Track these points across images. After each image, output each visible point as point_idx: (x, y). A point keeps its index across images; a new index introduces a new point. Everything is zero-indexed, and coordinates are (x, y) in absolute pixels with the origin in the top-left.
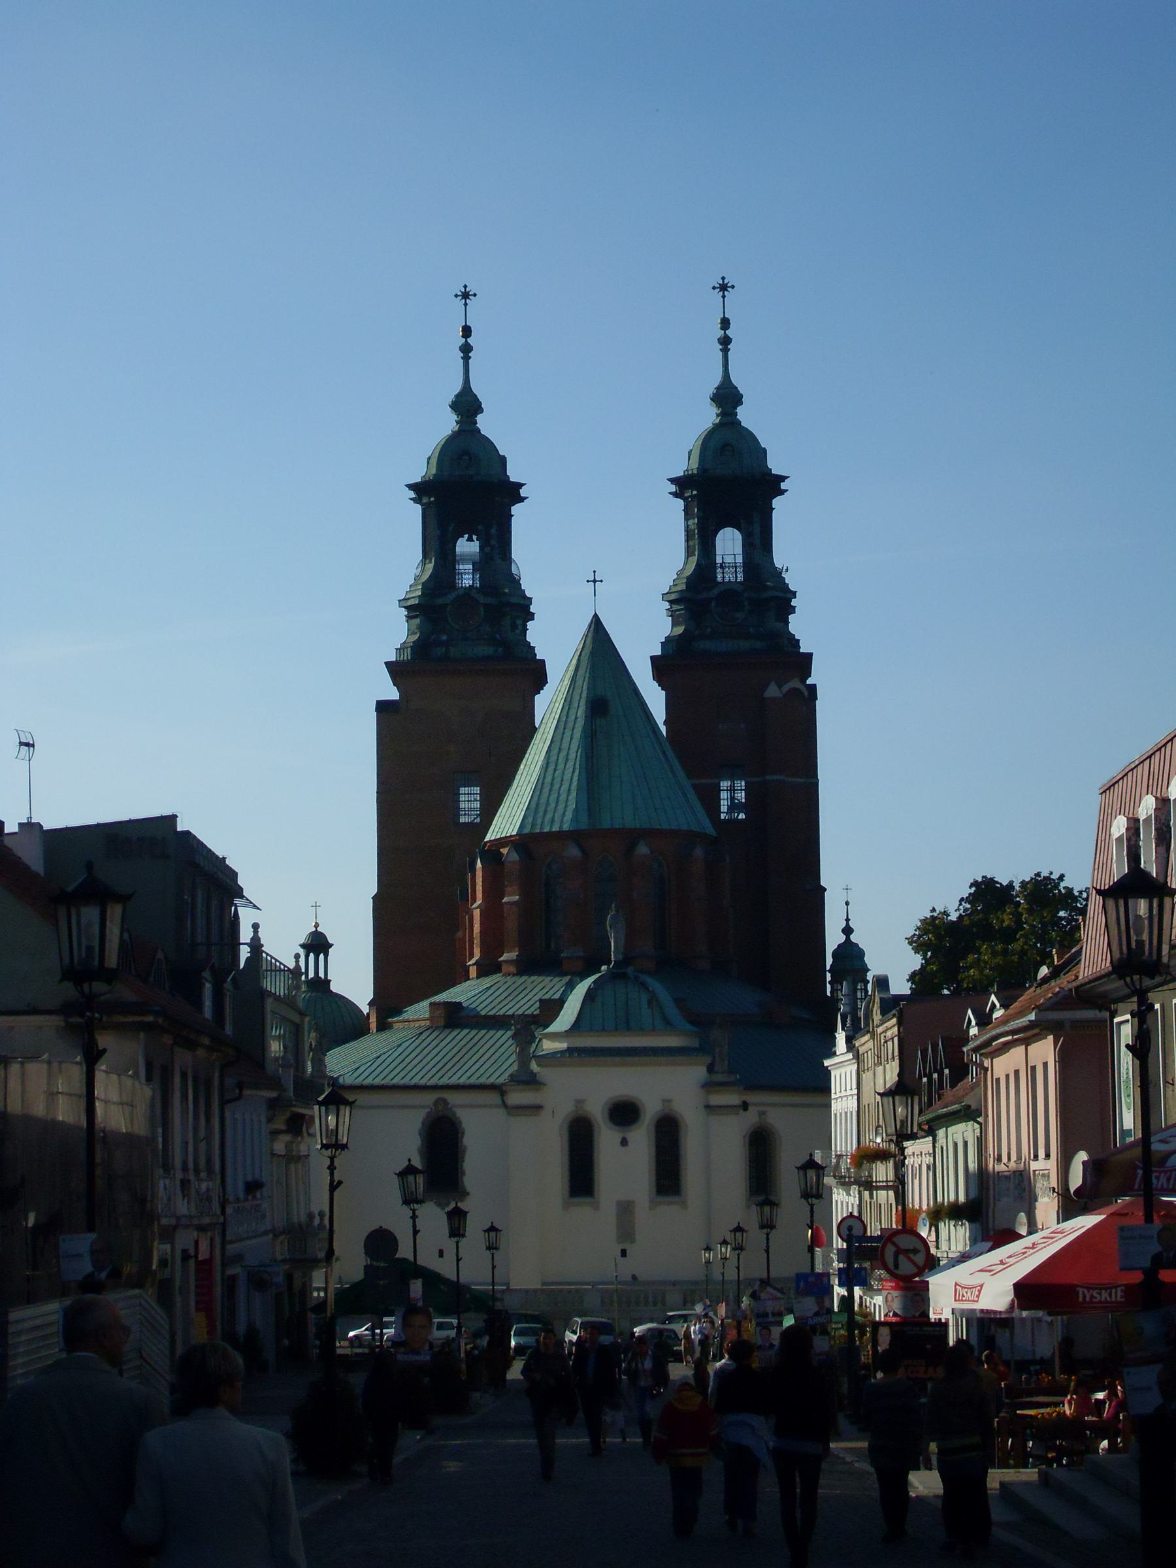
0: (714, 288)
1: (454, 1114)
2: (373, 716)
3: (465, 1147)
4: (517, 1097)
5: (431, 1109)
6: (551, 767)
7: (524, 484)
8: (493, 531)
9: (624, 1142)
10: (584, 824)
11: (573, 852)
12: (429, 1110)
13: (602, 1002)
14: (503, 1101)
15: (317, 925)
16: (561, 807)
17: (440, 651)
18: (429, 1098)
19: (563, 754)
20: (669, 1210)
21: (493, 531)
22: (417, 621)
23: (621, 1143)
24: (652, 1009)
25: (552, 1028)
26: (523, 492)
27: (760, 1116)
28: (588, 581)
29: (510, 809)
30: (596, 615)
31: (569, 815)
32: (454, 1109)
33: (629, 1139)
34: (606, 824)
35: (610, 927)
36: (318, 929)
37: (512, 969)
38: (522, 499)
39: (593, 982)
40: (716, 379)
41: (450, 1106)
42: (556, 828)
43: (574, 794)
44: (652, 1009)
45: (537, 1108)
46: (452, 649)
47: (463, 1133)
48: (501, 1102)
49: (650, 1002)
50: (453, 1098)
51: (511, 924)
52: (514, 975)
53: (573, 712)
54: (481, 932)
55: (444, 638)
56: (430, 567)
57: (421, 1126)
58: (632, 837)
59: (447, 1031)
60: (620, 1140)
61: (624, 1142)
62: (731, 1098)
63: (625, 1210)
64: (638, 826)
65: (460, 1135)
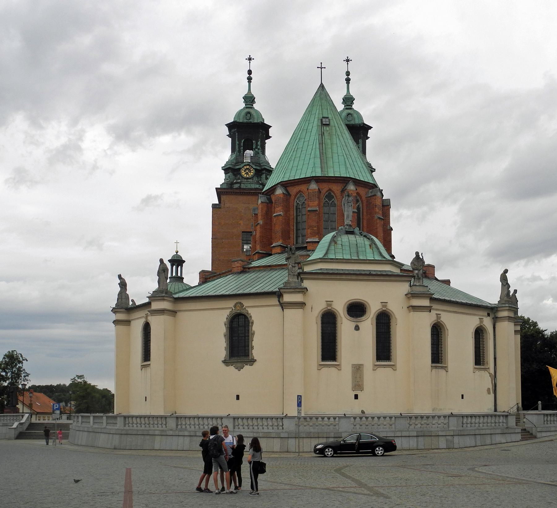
0: (344, 61)
2: (211, 209)
4: (287, 298)
5: (233, 309)
6: (300, 150)
7: (271, 127)
8: (259, 143)
9: (357, 328)
10: (319, 174)
11: (313, 186)
12: (231, 310)
13: (342, 245)
14: (279, 301)
15: (177, 252)
16: (306, 166)
17: (236, 186)
18: (231, 304)
19: (306, 143)
20: (384, 373)
21: (259, 143)
22: (229, 174)
23: (355, 328)
24: (373, 249)
26: (271, 132)
27: (437, 316)
28: (318, 68)
29: (277, 174)
30: (322, 86)
31: (310, 170)
36: (178, 254)
37: (278, 250)
38: (270, 137)
39: (336, 233)
40: (344, 93)
43: (312, 161)
44: (373, 249)
45: (302, 305)
46: (242, 185)
47: (252, 323)
48: (278, 303)
49: (370, 246)
50: (247, 303)
51: (278, 228)
52: (279, 253)
53: (311, 125)
54: (260, 237)
55: (239, 181)
56: (234, 156)
57: (225, 320)
58: (345, 181)
59: (241, 275)
60: (355, 326)
61: (357, 328)
62: (426, 302)
63: (358, 369)
64: (348, 176)
65: (250, 324)
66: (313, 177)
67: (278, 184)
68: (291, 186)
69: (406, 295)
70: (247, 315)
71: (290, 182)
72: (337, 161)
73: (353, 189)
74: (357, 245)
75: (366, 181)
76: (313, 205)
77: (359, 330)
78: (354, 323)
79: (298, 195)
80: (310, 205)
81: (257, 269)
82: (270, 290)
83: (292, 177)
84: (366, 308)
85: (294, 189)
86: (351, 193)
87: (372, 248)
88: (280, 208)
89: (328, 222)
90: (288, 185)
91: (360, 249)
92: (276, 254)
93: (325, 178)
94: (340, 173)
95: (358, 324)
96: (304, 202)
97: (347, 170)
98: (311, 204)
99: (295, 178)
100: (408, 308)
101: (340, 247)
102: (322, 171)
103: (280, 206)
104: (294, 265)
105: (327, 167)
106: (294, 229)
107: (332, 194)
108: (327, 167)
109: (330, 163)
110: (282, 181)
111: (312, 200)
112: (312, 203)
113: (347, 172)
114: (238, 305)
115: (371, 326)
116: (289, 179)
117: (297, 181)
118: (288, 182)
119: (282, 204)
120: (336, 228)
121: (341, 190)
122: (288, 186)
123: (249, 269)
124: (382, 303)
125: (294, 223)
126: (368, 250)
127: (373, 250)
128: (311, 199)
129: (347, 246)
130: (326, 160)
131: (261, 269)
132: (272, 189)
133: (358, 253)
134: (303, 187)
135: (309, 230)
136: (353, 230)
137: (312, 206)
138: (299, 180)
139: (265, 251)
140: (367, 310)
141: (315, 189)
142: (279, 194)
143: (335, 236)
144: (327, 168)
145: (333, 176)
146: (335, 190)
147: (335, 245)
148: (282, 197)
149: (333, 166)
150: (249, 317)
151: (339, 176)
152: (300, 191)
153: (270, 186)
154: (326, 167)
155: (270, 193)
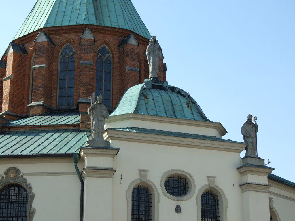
1: (26, 180)
3: (34, 210)
5: (3, 177)
9: (178, 209)
10: (93, 22)
11: (88, 35)
13: (153, 100)
24: (191, 109)
25: (117, 112)
32: (24, 177)
33: (182, 207)
34: (108, 24)
35: (149, 53)
37: (39, 110)
41: (21, 174)
42: (73, 23)
44: (191, 109)
45: (110, 171)
47: (33, 197)
48: (74, 170)
50: (24, 168)
52: (39, 115)
54: (10, 94)
60: (175, 207)
61: (178, 209)
64: (128, 29)
65: (29, 199)
66: (86, 25)
67: (38, 30)
68: (56, 34)
69: (237, 169)
70: (25, 186)
71: (55, 29)
72: (114, 10)
73: (134, 44)
74: (171, 101)
75: (146, 37)
76: (87, 58)
77: (181, 212)
78: (174, 202)
79: (64, 46)
80: (83, 57)
81: (22, 130)
82: (63, 151)
83: (58, 23)
84: (188, 184)
85: (59, 38)
86: (133, 49)
87: (189, 107)
88: (43, 59)
89: (102, 81)
90: (51, 33)
91: (176, 108)
92: (36, 115)
93: (101, 28)
94: (118, 24)
95: (179, 203)
96: (72, 55)
97: (126, 22)
98: (85, 56)
99: (63, 25)
100: (240, 186)
101: (151, 102)
102: (97, 19)
103: (43, 56)
104: (100, 119)
105: (102, 15)
106: (57, 87)
107: (107, 48)
108: (102, 15)
109: (106, 12)
110: (45, 26)
111: (86, 52)
112: (86, 55)
113: (126, 24)
114: (12, 171)
115: (195, 208)
116: (55, 25)
117: (65, 28)
118: (53, 29)
119: (46, 54)
120: (111, 90)
121: (118, 45)
122: (51, 34)
123: (9, 129)
124: (208, 177)
125: (57, 79)
126: (187, 110)
127: (191, 110)
128: (84, 51)
129: (160, 102)
130: (101, 7)
131: (27, 129)
132: (29, 36)
133: (174, 112)
134: (72, 37)
135: (82, 88)
136: (161, 84)
137: (86, 59)
138: (68, 28)
139: (15, 113)
140: (189, 186)
141: (90, 39)
142: (43, 42)
143: (145, 88)
144: (103, 17)
145: (110, 26)
146: (111, 43)
147: (145, 99)
148: (46, 45)
149: (109, 15)
150: (27, 189)
151: (118, 27)
152: (67, 41)
153: (27, 33)
154: (101, 16)
155: (24, 42)
